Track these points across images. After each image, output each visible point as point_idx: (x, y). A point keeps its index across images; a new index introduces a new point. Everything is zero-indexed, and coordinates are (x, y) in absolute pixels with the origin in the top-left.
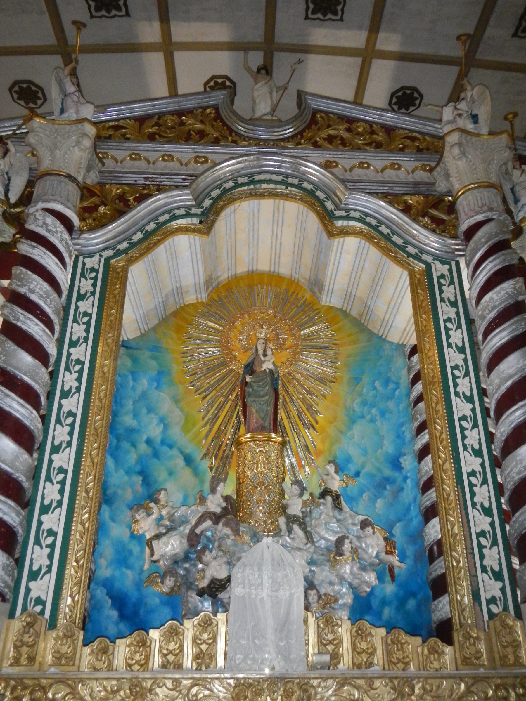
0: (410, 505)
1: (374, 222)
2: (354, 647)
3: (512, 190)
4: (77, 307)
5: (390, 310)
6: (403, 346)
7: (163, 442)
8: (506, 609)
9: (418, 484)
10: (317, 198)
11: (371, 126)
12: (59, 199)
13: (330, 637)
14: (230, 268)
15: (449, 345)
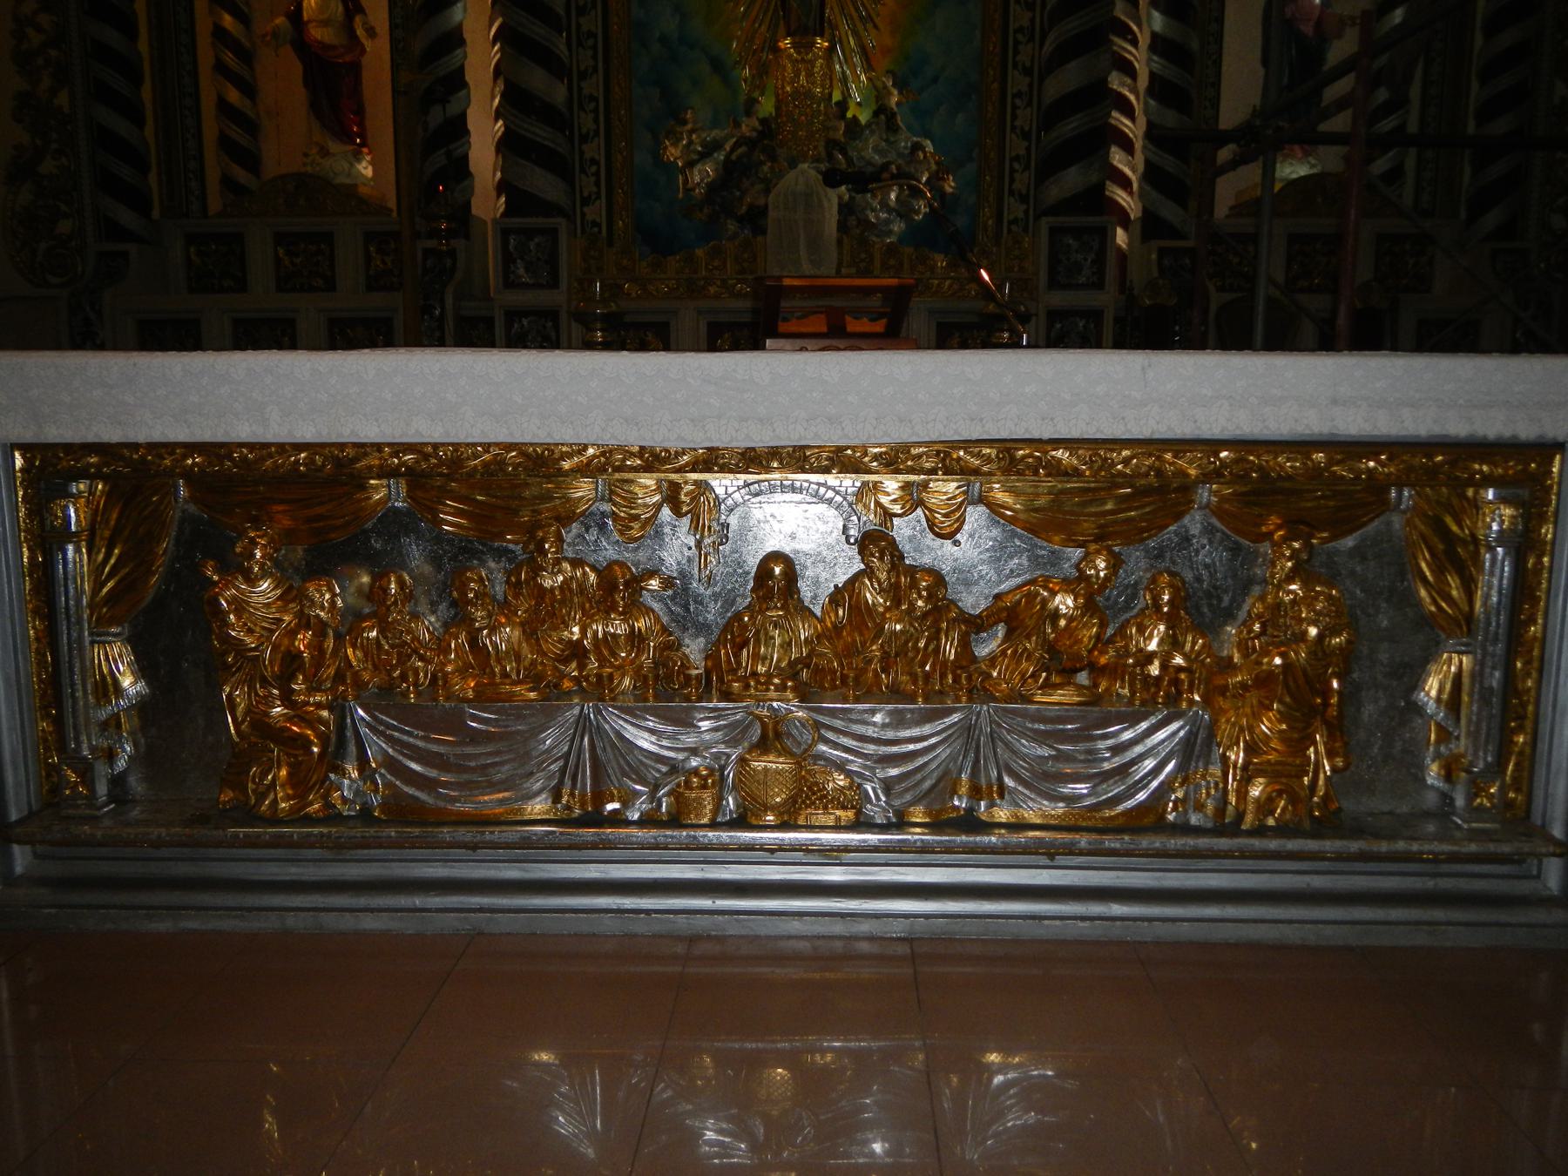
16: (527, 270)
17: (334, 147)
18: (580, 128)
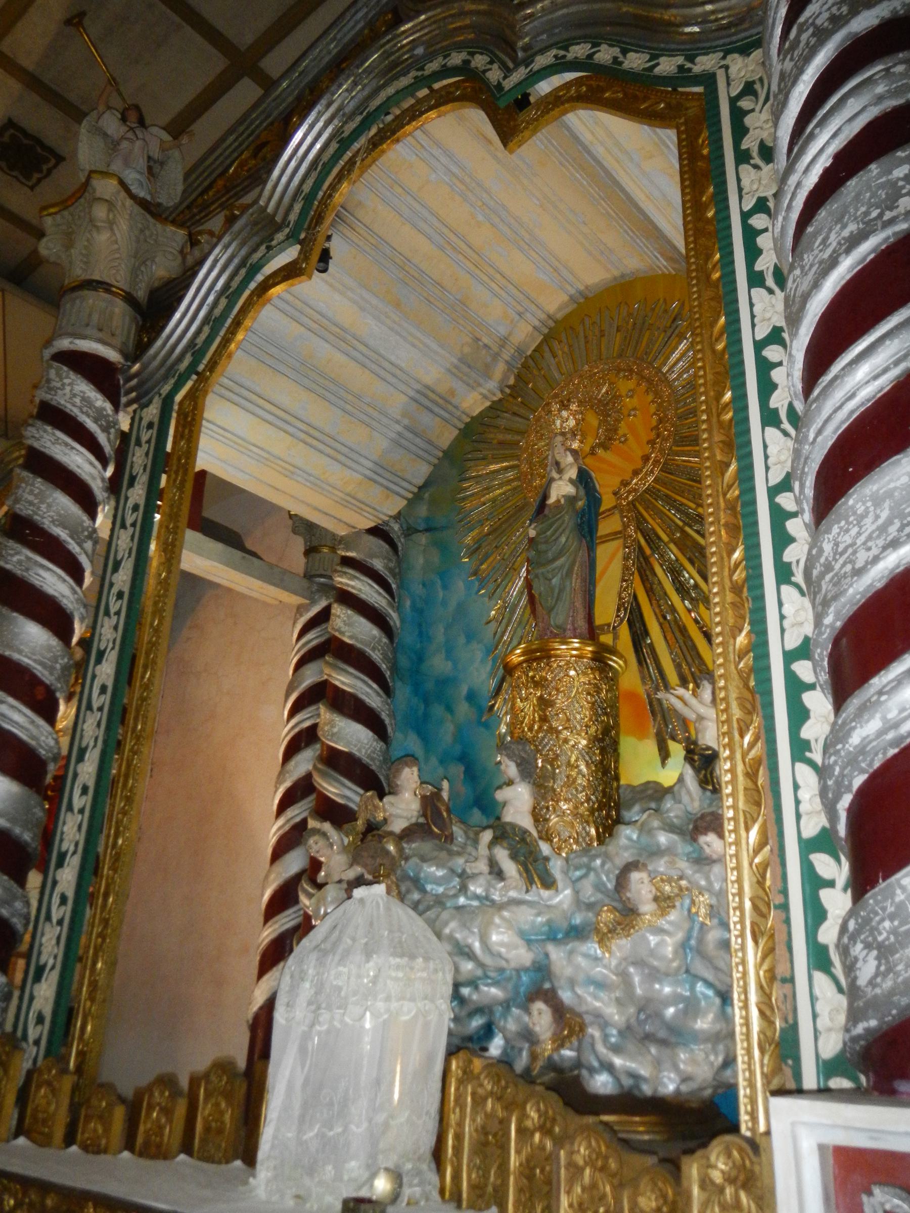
14: (521, 309)
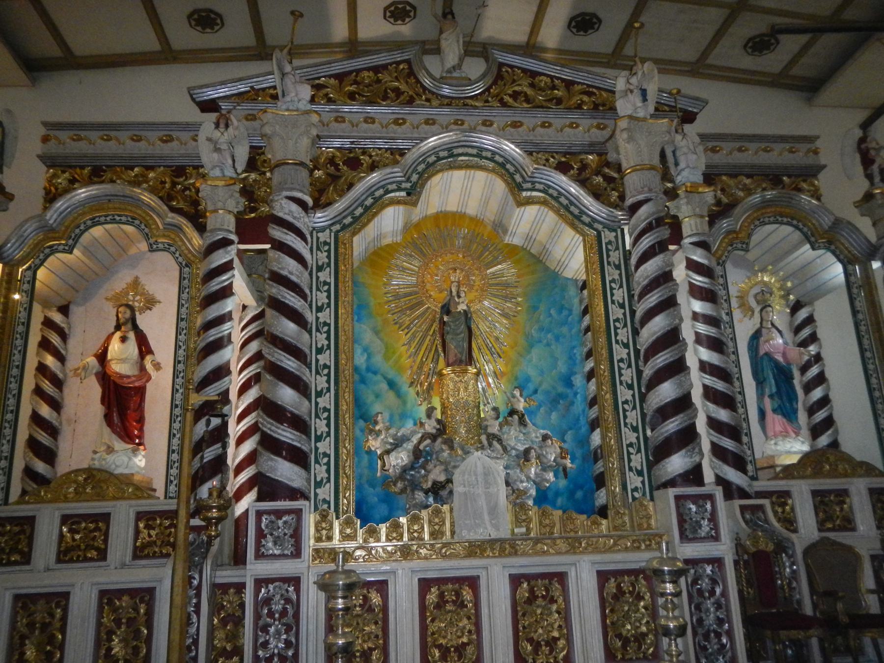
0: (579, 417)
1: (555, 194)
2: (541, 523)
3: (674, 152)
4: (318, 278)
5: (566, 255)
6: (576, 281)
7: (368, 369)
8: (644, 494)
9: (586, 398)
10: (507, 170)
11: (552, 81)
12: (298, 187)
13: (524, 517)
15: (613, 302)
16: (275, 543)
17: (119, 445)
18: (316, 431)
